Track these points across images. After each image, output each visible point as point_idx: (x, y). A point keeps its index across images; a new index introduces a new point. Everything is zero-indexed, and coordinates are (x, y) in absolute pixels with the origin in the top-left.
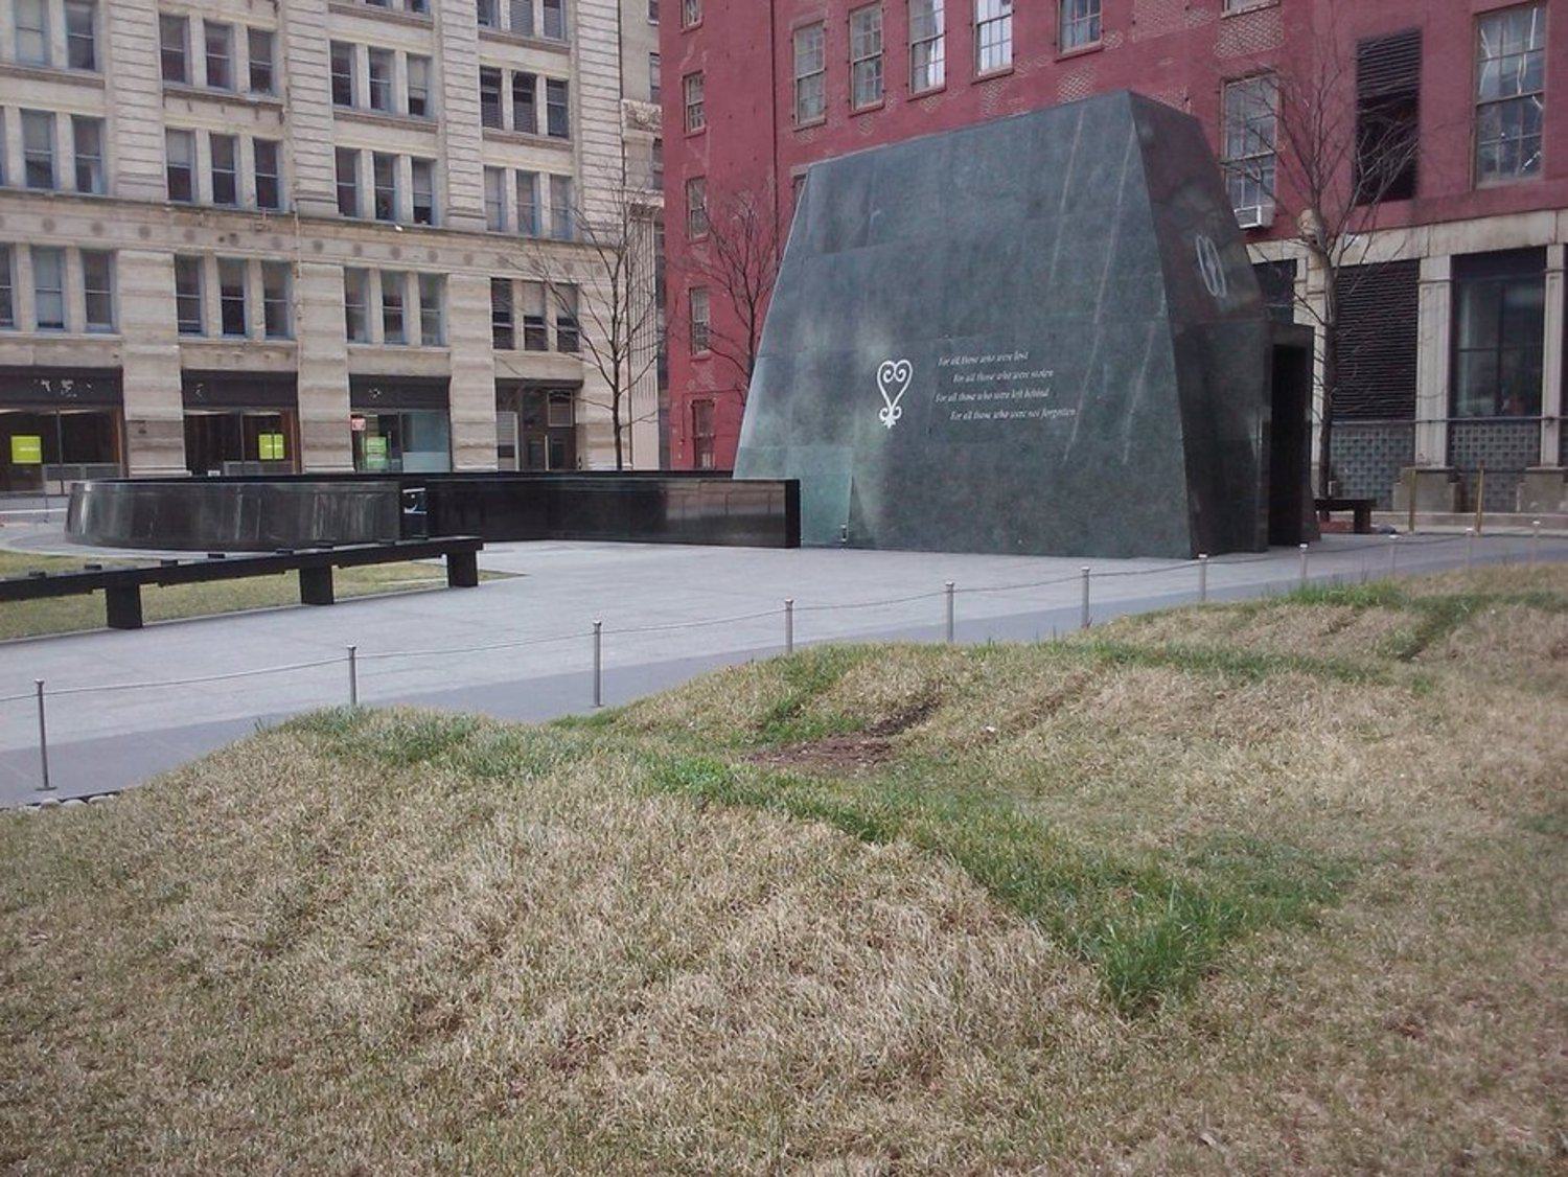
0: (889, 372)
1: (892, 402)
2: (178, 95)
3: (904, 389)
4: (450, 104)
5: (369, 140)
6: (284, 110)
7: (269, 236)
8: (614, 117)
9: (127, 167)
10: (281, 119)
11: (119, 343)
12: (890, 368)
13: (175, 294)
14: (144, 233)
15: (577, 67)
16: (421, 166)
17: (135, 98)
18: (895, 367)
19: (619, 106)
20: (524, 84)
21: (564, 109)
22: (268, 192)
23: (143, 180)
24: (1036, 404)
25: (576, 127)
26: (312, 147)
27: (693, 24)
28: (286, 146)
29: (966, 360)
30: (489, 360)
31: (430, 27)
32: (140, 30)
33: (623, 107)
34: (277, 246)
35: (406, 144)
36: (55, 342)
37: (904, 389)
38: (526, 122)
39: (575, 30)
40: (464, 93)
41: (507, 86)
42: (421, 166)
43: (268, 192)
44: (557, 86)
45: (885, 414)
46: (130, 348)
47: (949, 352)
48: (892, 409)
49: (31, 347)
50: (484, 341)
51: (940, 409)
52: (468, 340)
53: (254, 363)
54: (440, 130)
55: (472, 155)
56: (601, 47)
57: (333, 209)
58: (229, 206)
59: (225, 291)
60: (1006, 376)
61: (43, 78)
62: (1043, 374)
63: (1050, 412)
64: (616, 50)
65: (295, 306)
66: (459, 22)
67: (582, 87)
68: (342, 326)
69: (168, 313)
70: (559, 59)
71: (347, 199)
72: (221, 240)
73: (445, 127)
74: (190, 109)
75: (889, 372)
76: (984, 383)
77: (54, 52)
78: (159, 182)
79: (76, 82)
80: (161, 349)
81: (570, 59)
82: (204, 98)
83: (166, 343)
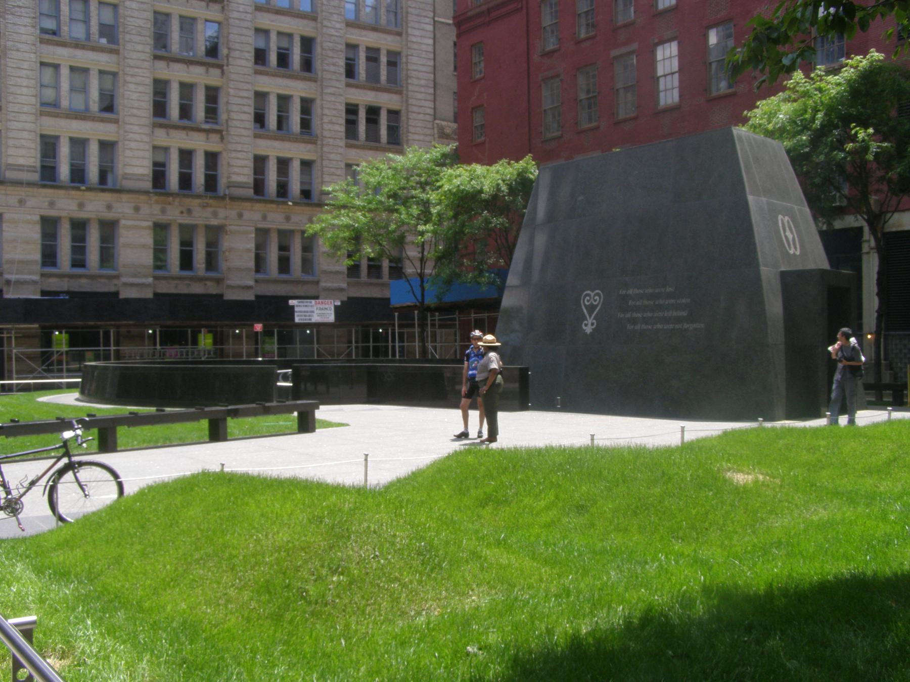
1: (590, 316)
2: (161, 126)
3: (597, 309)
4: (326, 127)
5: (273, 149)
6: (224, 133)
7: (211, 210)
8: (428, 132)
9: (129, 170)
10: (222, 138)
11: (117, 277)
12: (588, 295)
13: (152, 246)
14: (137, 209)
15: (407, 101)
16: (306, 165)
17: (136, 128)
18: (592, 294)
19: (433, 125)
20: (373, 113)
21: (397, 127)
22: (211, 183)
23: (140, 178)
24: (679, 320)
25: (405, 138)
26: (240, 155)
27: (478, 76)
28: (224, 154)
29: (637, 291)
30: (344, 285)
31: (316, 81)
32: (141, 88)
33: (435, 125)
34: (215, 214)
35: (297, 152)
36: (80, 276)
37: (597, 309)
38: (373, 136)
39: (407, 80)
40: (334, 119)
41: (362, 115)
42: (306, 165)
43: (211, 183)
44: (394, 114)
45: (586, 325)
46: (124, 280)
49: (66, 280)
50: (344, 273)
52: (331, 272)
53: (197, 289)
54: (319, 142)
55: (338, 157)
56: (423, 90)
57: (251, 192)
58: (186, 192)
59: (183, 244)
60: (661, 302)
61: (84, 118)
62: (684, 301)
63: (688, 326)
64: (431, 91)
65: (224, 252)
66: (334, 77)
67: (410, 114)
68: (252, 264)
69: (147, 258)
70: (395, 97)
71: (259, 186)
72: (182, 212)
73: (322, 141)
74: (168, 134)
75: (588, 298)
77: (91, 103)
78: (146, 178)
79: (102, 120)
80: (143, 281)
81: (402, 97)
82: (176, 127)
83: (146, 276)
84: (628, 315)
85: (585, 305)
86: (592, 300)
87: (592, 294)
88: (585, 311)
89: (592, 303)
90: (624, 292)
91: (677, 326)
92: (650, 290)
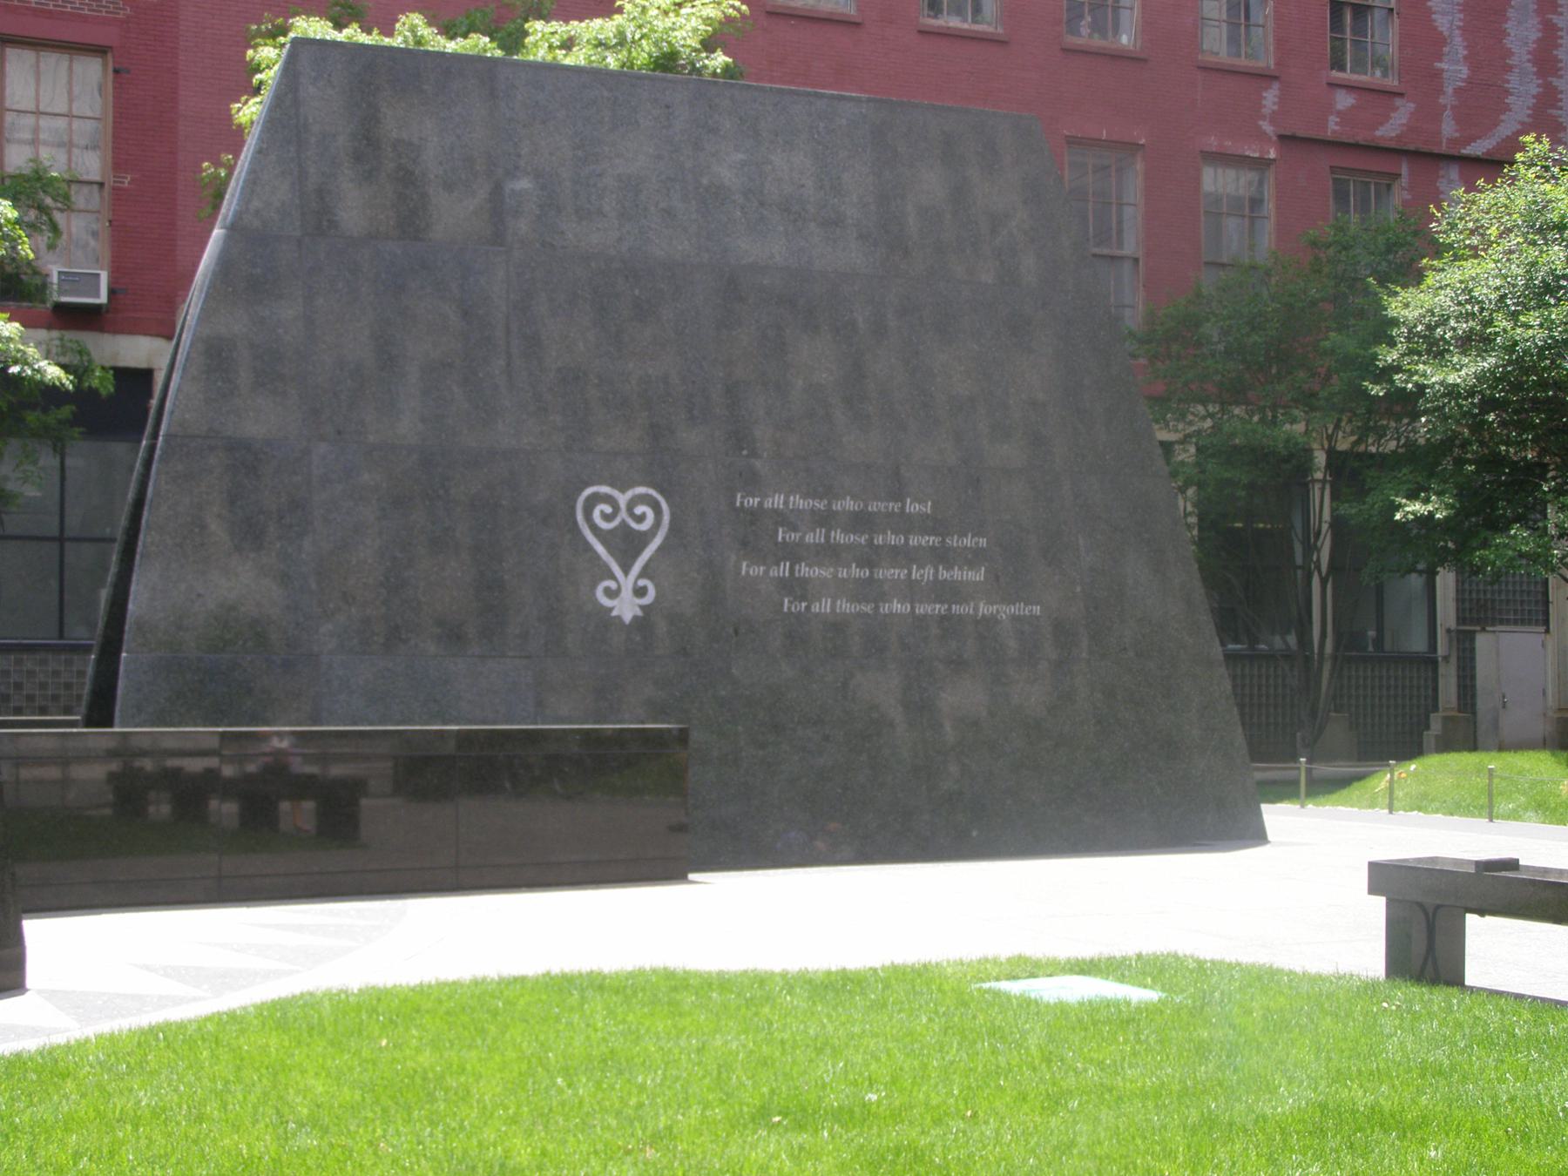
0: (608, 509)
1: (626, 571)
12: (609, 499)
18: (623, 499)
48: (627, 583)
75: (608, 509)
76: (849, 547)
84: (783, 570)
85: (595, 529)
86: (623, 514)
88: (600, 549)
89: (624, 524)
90: (753, 502)
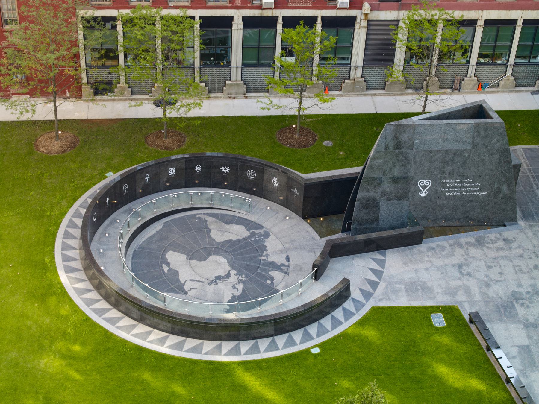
12: (423, 182)
24: (474, 191)
47: (445, 178)
48: (424, 192)
51: (442, 191)
62: (477, 184)
85: (420, 185)
86: (425, 183)
87: (425, 181)
91: (473, 193)
92: (459, 180)
